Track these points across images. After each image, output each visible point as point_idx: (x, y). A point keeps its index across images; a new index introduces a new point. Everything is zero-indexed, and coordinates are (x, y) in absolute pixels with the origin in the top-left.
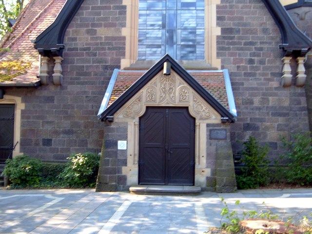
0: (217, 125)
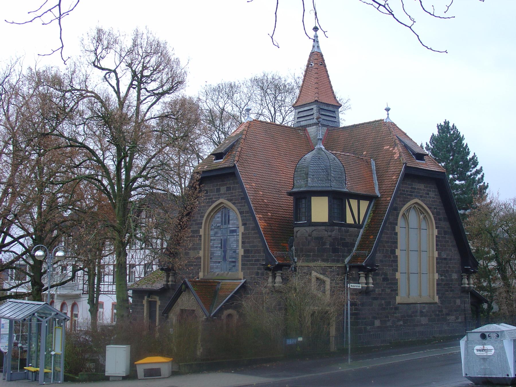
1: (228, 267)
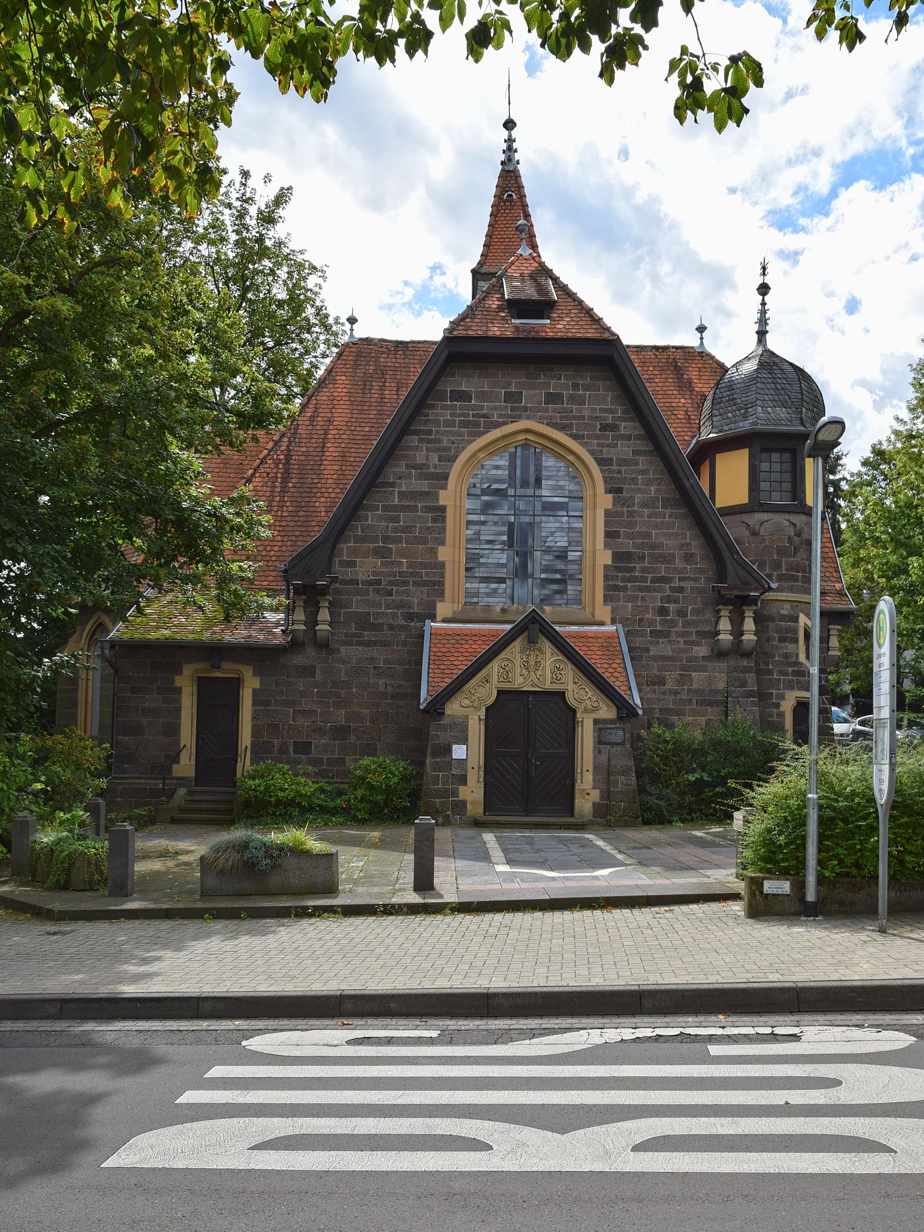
0: (611, 721)
1: (536, 592)
